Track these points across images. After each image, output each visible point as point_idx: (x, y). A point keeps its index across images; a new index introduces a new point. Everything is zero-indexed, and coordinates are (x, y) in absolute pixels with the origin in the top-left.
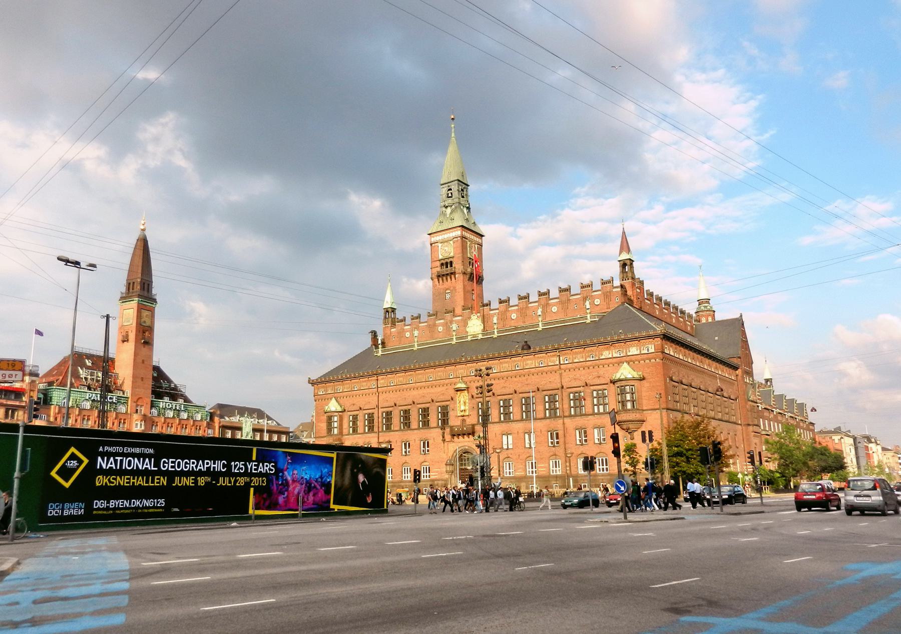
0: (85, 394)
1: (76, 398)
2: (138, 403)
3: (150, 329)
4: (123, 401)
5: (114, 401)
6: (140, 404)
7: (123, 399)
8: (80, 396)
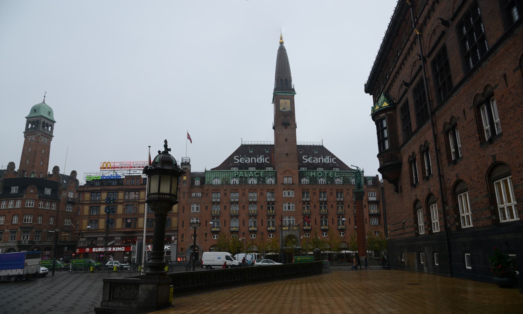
0: (233, 173)
1: (225, 177)
2: (285, 175)
3: (291, 114)
4: (270, 175)
5: (261, 176)
6: (288, 175)
7: (270, 173)
8: (229, 175)
